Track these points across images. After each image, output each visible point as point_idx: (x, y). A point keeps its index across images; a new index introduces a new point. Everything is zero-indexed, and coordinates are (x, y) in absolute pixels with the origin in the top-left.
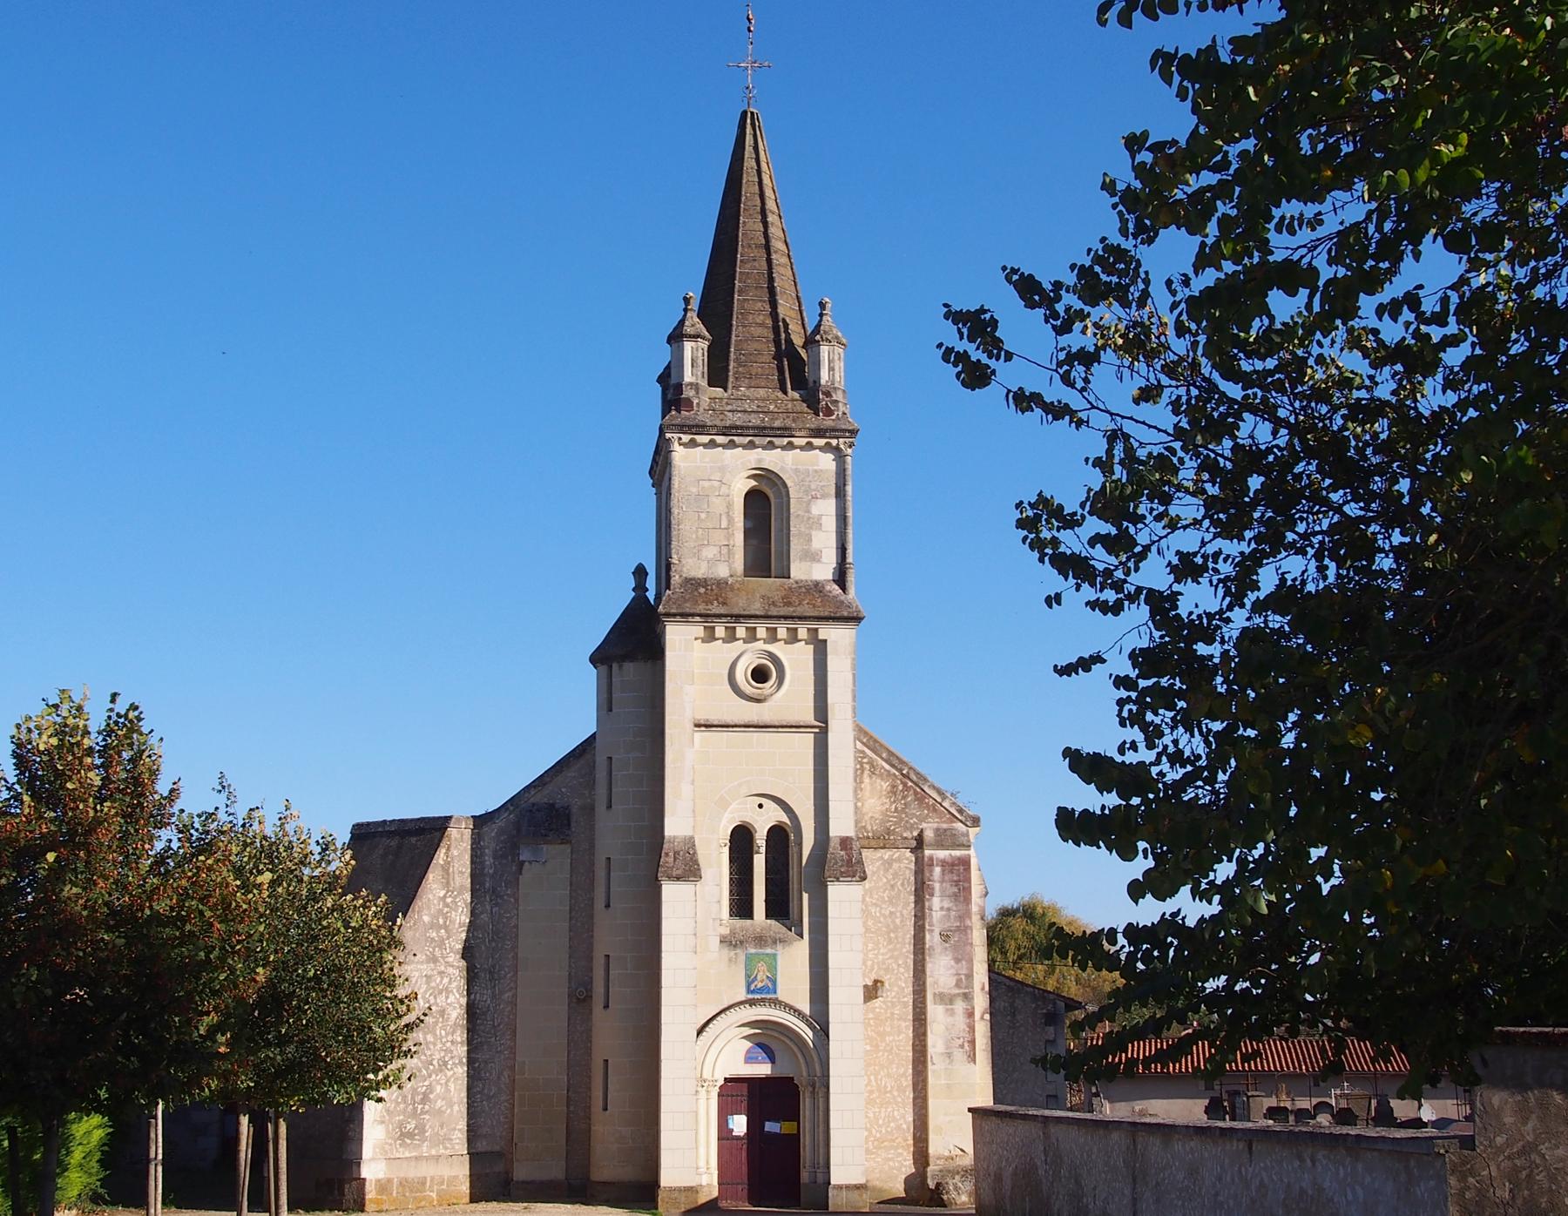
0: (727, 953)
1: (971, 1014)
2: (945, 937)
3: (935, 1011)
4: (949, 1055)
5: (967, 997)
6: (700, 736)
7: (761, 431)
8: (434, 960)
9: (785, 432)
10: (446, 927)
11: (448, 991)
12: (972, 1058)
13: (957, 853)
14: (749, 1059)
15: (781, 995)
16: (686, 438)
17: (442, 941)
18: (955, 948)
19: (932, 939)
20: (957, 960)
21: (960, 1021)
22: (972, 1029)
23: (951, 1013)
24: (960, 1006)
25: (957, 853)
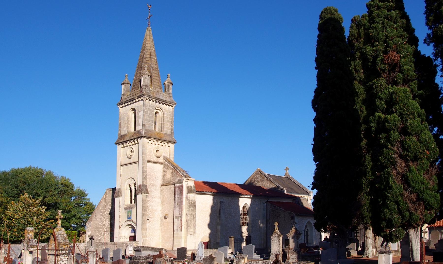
0: (125, 211)
1: (181, 221)
2: (178, 204)
3: (176, 220)
4: (177, 230)
5: (181, 217)
6: (122, 167)
7: (131, 100)
8: (102, 215)
9: (134, 99)
10: (105, 209)
11: (105, 221)
12: (181, 230)
13: (181, 184)
14: (131, 232)
15: (132, 219)
16: (121, 106)
17: (104, 212)
18: (179, 206)
19: (176, 204)
20: (180, 209)
21: (180, 222)
22: (182, 224)
23: (178, 220)
24: (180, 219)
25: (181, 184)
